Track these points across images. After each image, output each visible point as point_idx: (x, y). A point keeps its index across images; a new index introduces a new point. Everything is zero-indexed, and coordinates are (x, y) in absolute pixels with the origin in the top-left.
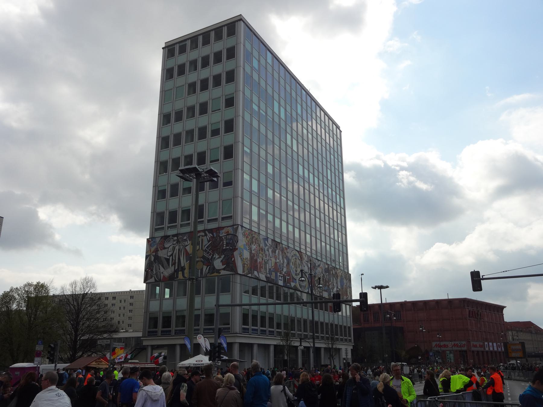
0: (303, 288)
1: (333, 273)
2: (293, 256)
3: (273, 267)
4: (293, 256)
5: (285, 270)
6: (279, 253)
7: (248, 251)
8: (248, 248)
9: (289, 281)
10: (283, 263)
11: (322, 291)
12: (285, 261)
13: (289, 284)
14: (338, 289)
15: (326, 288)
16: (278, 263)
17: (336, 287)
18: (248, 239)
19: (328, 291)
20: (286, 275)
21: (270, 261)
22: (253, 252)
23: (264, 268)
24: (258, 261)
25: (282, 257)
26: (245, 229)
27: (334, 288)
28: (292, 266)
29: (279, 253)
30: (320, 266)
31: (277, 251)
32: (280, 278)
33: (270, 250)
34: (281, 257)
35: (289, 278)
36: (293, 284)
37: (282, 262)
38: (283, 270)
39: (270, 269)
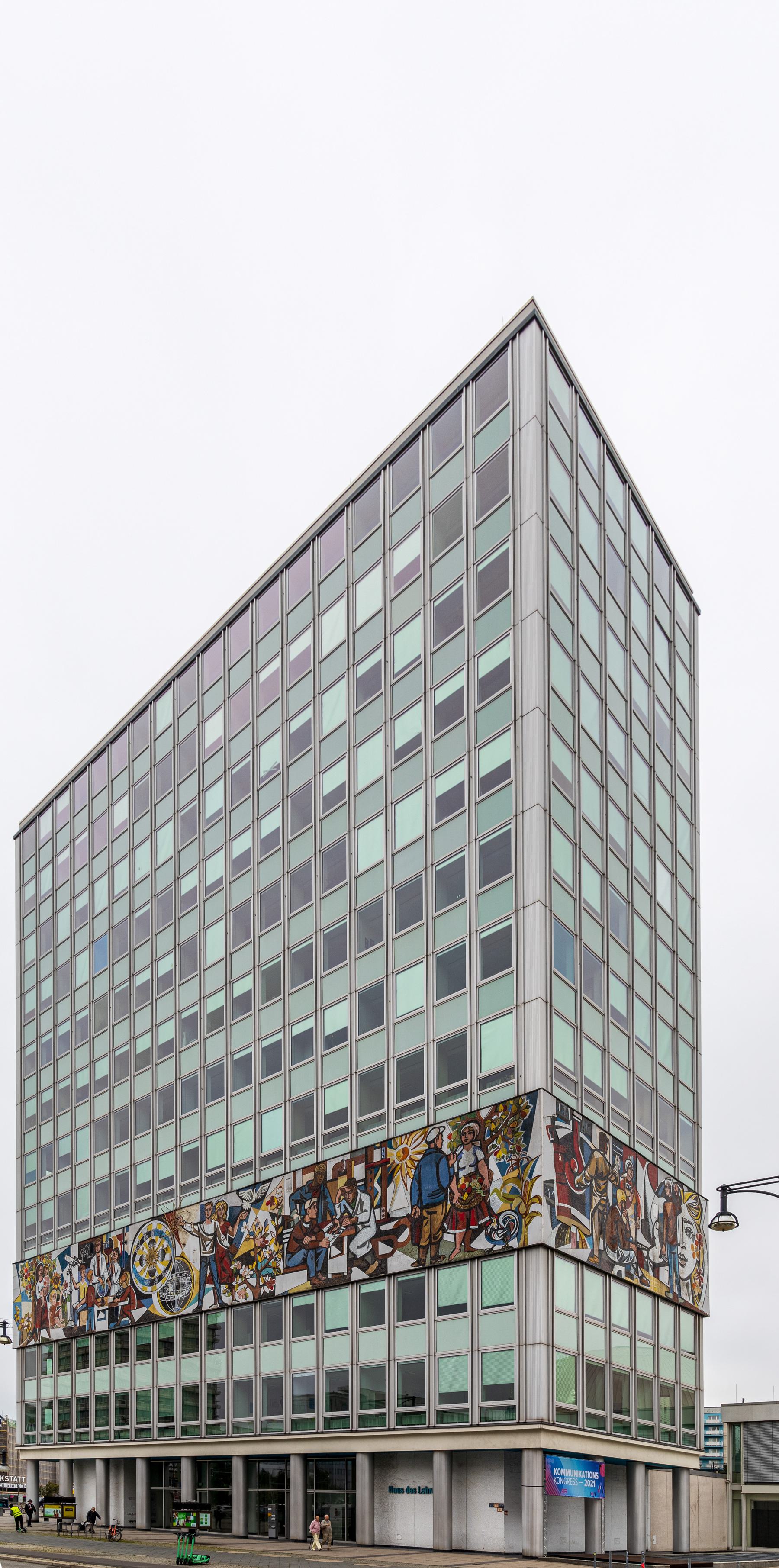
0: (175, 1309)
1: (352, 1182)
2: (142, 1242)
3: (84, 1301)
4: (142, 1242)
5: (115, 1290)
6: (98, 1261)
7: (30, 1301)
8: (29, 1295)
9: (127, 1311)
10: (111, 1276)
11: (273, 1277)
12: (117, 1267)
13: (127, 1319)
14: (390, 1226)
15: (299, 1256)
16: (95, 1286)
17: (372, 1223)
18: (29, 1279)
19: (311, 1263)
20: (117, 1300)
21: (75, 1293)
22: (38, 1296)
23: (60, 1314)
24: (49, 1305)
25: (107, 1264)
26: (22, 1264)
27: (351, 1239)
28: (139, 1269)
29: (98, 1261)
30: (268, 1199)
31: (94, 1260)
32: (101, 1315)
33: (75, 1270)
34: (104, 1267)
35: (126, 1303)
36: (138, 1314)
37: (106, 1276)
38: (108, 1294)
39: (74, 1310)
